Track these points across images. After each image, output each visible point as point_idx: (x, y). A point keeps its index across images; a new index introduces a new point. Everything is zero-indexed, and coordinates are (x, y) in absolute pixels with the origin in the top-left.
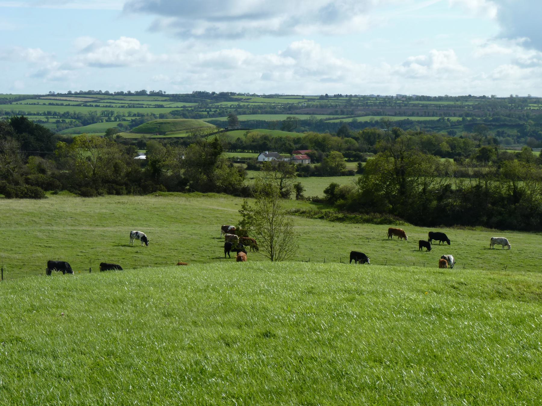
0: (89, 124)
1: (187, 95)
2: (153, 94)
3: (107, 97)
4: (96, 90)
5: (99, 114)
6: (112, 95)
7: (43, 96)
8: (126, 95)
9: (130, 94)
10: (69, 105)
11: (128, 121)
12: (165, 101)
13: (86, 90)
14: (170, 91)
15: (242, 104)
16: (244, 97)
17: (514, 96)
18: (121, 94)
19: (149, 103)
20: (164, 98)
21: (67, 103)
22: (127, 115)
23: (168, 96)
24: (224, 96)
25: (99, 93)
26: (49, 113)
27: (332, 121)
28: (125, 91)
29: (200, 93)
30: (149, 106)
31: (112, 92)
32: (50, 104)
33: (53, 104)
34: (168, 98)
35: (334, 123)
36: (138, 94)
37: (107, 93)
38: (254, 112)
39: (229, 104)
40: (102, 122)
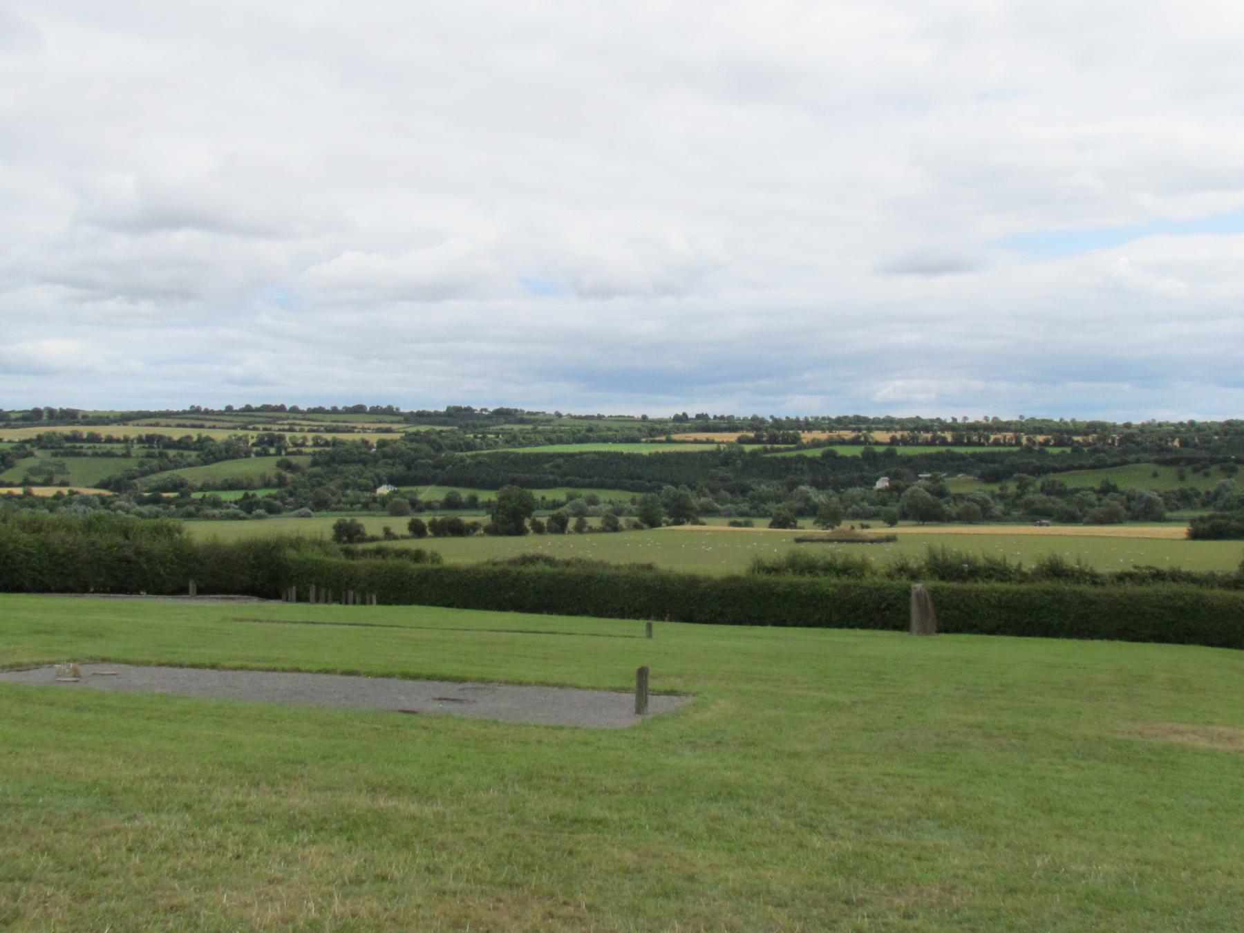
0: (217, 460)
1: (437, 414)
2: (375, 411)
3: (292, 415)
5: (251, 441)
6: (302, 412)
7: (178, 413)
8: (327, 412)
9: (335, 411)
10: (214, 427)
11: (306, 454)
12: (399, 422)
13: (256, 404)
15: (540, 428)
16: (540, 417)
17: (960, 420)
18: (320, 410)
19: (366, 426)
20: (395, 418)
22: (310, 443)
24: (504, 415)
25: (281, 408)
26: (150, 439)
27: (779, 455)
28: (328, 407)
29: (458, 410)
30: (364, 430)
31: (303, 407)
32: (179, 426)
33: (184, 426)
35: (784, 458)
36: (348, 411)
37: (294, 410)
38: (560, 441)
39: (517, 427)
40: (247, 455)
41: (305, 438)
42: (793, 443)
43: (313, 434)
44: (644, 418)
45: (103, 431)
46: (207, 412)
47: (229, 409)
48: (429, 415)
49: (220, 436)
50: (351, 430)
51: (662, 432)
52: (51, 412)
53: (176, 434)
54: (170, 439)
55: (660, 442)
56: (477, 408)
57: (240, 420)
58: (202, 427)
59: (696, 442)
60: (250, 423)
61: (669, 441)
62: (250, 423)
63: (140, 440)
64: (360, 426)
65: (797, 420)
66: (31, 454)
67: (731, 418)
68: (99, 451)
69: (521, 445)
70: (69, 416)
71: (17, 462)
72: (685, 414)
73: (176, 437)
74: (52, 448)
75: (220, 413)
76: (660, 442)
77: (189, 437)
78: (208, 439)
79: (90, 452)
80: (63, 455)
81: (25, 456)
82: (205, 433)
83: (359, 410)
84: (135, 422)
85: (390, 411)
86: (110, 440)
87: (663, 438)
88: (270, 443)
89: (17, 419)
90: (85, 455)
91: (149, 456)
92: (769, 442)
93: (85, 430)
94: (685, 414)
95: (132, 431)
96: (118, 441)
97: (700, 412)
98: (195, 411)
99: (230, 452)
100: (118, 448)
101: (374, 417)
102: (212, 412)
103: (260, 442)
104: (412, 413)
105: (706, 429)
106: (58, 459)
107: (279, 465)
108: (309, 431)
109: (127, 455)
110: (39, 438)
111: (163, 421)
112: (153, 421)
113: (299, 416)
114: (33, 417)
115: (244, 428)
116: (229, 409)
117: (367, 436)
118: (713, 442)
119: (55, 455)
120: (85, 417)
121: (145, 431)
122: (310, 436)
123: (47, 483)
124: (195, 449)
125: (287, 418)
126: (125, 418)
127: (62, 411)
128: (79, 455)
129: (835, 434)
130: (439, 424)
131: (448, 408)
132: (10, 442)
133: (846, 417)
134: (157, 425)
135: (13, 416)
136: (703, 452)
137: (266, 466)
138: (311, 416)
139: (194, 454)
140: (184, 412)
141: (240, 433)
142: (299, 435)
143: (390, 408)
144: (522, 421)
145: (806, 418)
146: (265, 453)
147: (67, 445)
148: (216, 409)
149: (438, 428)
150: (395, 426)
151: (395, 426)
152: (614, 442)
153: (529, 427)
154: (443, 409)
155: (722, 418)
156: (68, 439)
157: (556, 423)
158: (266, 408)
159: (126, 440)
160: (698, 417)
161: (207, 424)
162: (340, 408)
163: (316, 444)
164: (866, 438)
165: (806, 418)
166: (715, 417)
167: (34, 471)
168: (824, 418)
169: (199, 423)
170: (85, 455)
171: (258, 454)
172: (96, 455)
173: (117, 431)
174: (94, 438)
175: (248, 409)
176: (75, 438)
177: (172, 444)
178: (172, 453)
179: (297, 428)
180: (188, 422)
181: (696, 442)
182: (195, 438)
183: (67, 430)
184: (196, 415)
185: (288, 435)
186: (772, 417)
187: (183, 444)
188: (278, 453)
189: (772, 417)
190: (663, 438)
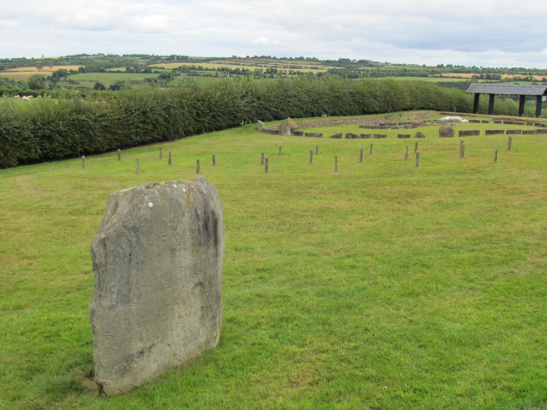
1: (335, 62)
2: (308, 59)
3: (274, 61)
4: (267, 55)
6: (278, 59)
7: (228, 58)
8: (288, 60)
9: (291, 59)
13: (259, 55)
14: (322, 58)
18: (285, 59)
19: (306, 66)
21: (243, 63)
22: (288, 73)
23: (320, 61)
25: (269, 57)
26: (223, 69)
28: (288, 57)
30: (306, 68)
31: (278, 57)
34: (320, 63)
36: (297, 59)
39: (370, 69)
41: (286, 71)
42: (497, 79)
43: (290, 69)
44: (424, 66)
45: (204, 65)
46: (239, 58)
47: (248, 57)
48: (331, 62)
50: (300, 68)
51: (437, 72)
52: (178, 57)
53: (233, 68)
54: (231, 69)
55: (437, 77)
56: (351, 59)
57: (253, 62)
58: (239, 64)
59: (453, 77)
60: (258, 63)
61: (441, 77)
62: (258, 63)
64: (303, 66)
65: (493, 69)
67: (462, 67)
68: (206, 74)
69: (377, 77)
70: (185, 59)
71: (175, 77)
72: (442, 65)
74: (186, 72)
75: (244, 59)
76: (437, 77)
77: (238, 69)
78: (247, 70)
79: (202, 74)
80: (191, 75)
81: (177, 75)
82: (246, 68)
83: (301, 59)
84: (212, 62)
85: (314, 60)
86: (207, 69)
87: (438, 75)
88: (272, 72)
89: (165, 59)
90: (200, 76)
92: (486, 79)
93: (197, 65)
94: (442, 65)
95: (216, 66)
97: (448, 64)
98: (234, 57)
100: (214, 73)
101: (309, 62)
102: (241, 59)
103: (268, 72)
104: (324, 61)
105: (456, 72)
106: (190, 77)
108: (283, 68)
109: (217, 76)
110: (180, 68)
112: (219, 61)
113: (277, 61)
114: (171, 59)
115: (257, 66)
116: (248, 57)
117: (312, 71)
118: (461, 78)
119: (189, 75)
120: (191, 59)
121: (221, 66)
122: (288, 70)
124: (242, 74)
125: (272, 62)
126: (207, 60)
127: (183, 56)
128: (198, 75)
129: (517, 76)
130: (336, 66)
131: (340, 59)
132: (168, 69)
133: (516, 68)
134: (221, 63)
135: (163, 58)
136: (460, 82)
138: (281, 61)
140: (230, 58)
142: (284, 69)
143: (314, 58)
144: (371, 66)
145: (497, 68)
147: (192, 71)
148: (243, 57)
149: (337, 68)
150: (318, 67)
151: (318, 67)
152: (416, 76)
153: (376, 68)
154: (337, 60)
155: (458, 66)
157: (386, 67)
158: (263, 57)
160: (448, 66)
161: (241, 63)
162: (293, 58)
163: (290, 74)
164: (531, 79)
165: (497, 68)
166: (455, 66)
168: (505, 68)
169: (238, 63)
170: (200, 76)
172: (204, 76)
173: (210, 66)
174: (200, 69)
175: (256, 57)
176: (193, 68)
179: (278, 66)
180: (234, 63)
181: (453, 77)
182: (241, 70)
183: (190, 65)
184: (235, 60)
186: (481, 67)
189: (481, 67)
190: (438, 75)
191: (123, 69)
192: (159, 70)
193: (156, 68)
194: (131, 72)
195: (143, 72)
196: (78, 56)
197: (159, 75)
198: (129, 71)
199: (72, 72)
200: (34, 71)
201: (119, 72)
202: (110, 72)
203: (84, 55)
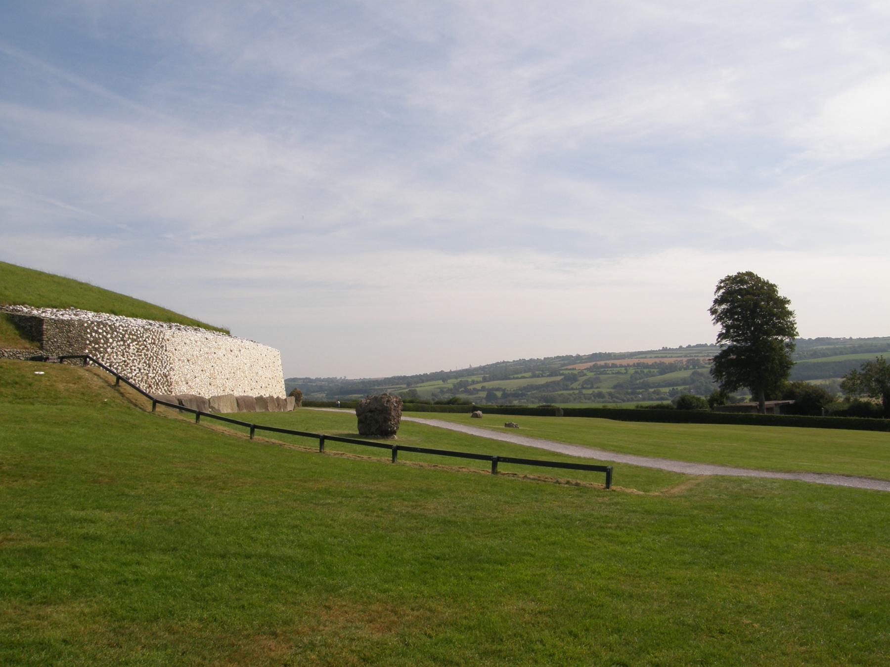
26: (639, 365)
40: (680, 370)
45: (618, 362)
47: (681, 347)
49: (667, 361)
53: (650, 361)
63: (634, 365)
66: (585, 375)
70: (608, 356)
73: (650, 363)
82: (663, 360)
86: (621, 366)
91: (636, 372)
93: (610, 362)
95: (631, 362)
96: (625, 366)
99: (672, 368)
107: (693, 374)
111: (649, 356)
115: (685, 356)
116: (681, 347)
121: (636, 361)
123: (592, 388)
134: (645, 358)
137: (686, 374)
139: (656, 370)
141: (679, 359)
144: (829, 344)
146: (687, 368)
156: (602, 367)
158: (698, 346)
159: (628, 366)
167: (585, 382)
171: (685, 369)
173: (624, 362)
174: (614, 366)
176: (606, 366)
177: (647, 366)
178: (646, 371)
183: (602, 363)
185: (701, 359)
187: (653, 366)
188: (694, 368)
191: (529, 374)
192: (566, 372)
193: (567, 369)
194: (538, 377)
195: (549, 376)
196: (498, 363)
197: (562, 377)
198: (534, 376)
199: (474, 382)
200: (440, 383)
201: (523, 377)
202: (514, 378)
203: (504, 362)
